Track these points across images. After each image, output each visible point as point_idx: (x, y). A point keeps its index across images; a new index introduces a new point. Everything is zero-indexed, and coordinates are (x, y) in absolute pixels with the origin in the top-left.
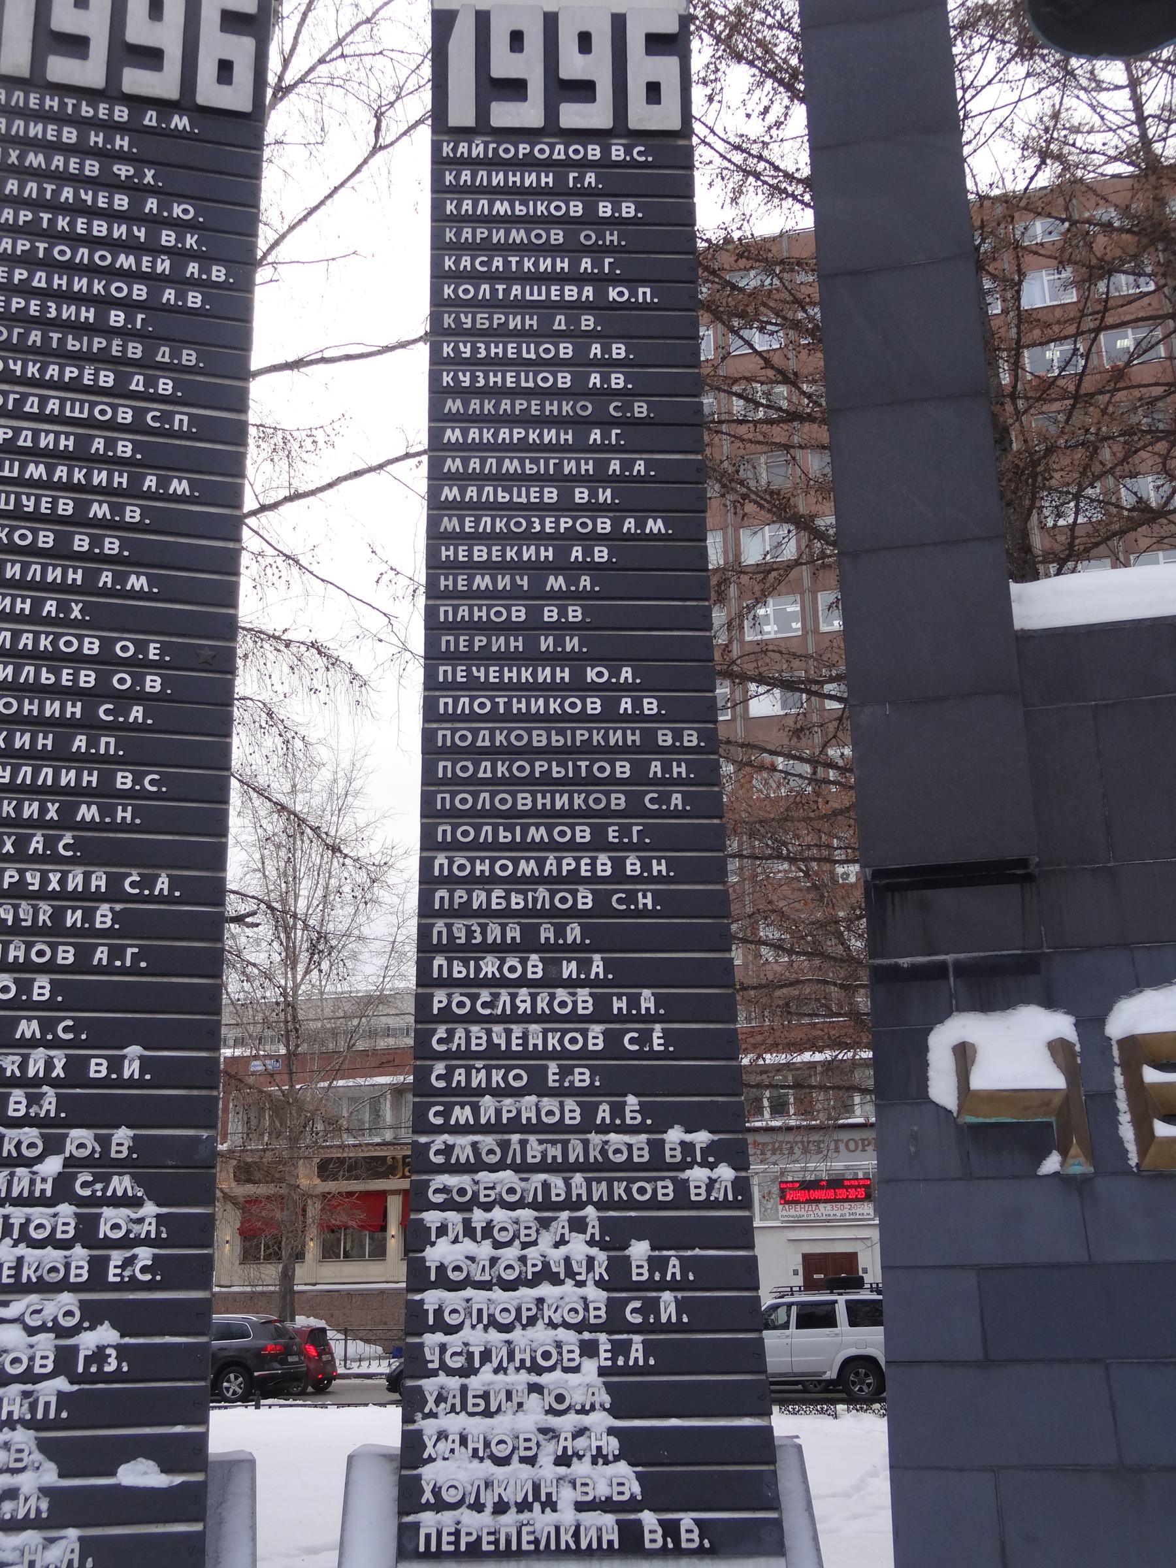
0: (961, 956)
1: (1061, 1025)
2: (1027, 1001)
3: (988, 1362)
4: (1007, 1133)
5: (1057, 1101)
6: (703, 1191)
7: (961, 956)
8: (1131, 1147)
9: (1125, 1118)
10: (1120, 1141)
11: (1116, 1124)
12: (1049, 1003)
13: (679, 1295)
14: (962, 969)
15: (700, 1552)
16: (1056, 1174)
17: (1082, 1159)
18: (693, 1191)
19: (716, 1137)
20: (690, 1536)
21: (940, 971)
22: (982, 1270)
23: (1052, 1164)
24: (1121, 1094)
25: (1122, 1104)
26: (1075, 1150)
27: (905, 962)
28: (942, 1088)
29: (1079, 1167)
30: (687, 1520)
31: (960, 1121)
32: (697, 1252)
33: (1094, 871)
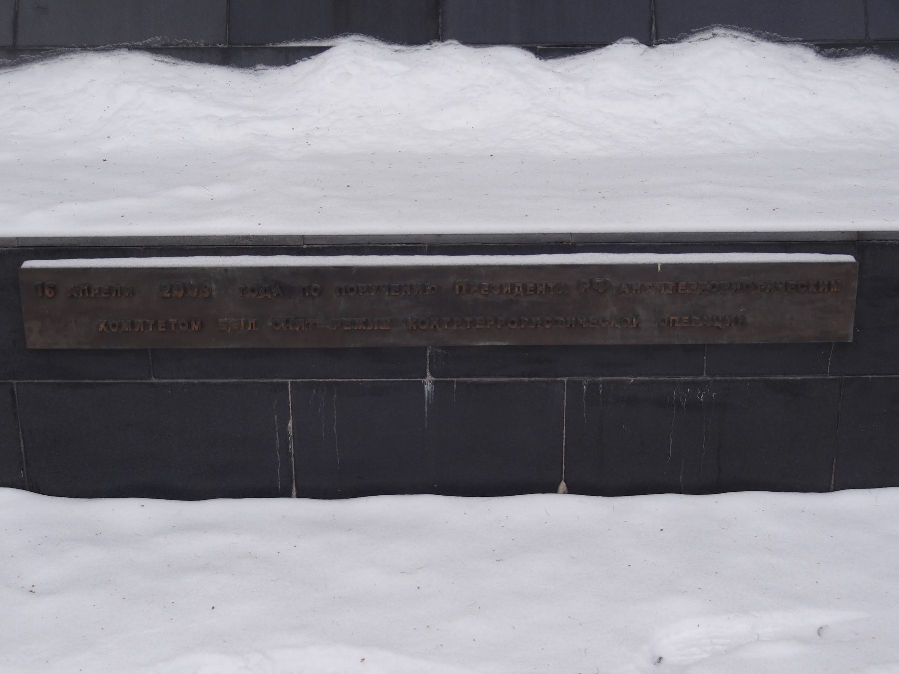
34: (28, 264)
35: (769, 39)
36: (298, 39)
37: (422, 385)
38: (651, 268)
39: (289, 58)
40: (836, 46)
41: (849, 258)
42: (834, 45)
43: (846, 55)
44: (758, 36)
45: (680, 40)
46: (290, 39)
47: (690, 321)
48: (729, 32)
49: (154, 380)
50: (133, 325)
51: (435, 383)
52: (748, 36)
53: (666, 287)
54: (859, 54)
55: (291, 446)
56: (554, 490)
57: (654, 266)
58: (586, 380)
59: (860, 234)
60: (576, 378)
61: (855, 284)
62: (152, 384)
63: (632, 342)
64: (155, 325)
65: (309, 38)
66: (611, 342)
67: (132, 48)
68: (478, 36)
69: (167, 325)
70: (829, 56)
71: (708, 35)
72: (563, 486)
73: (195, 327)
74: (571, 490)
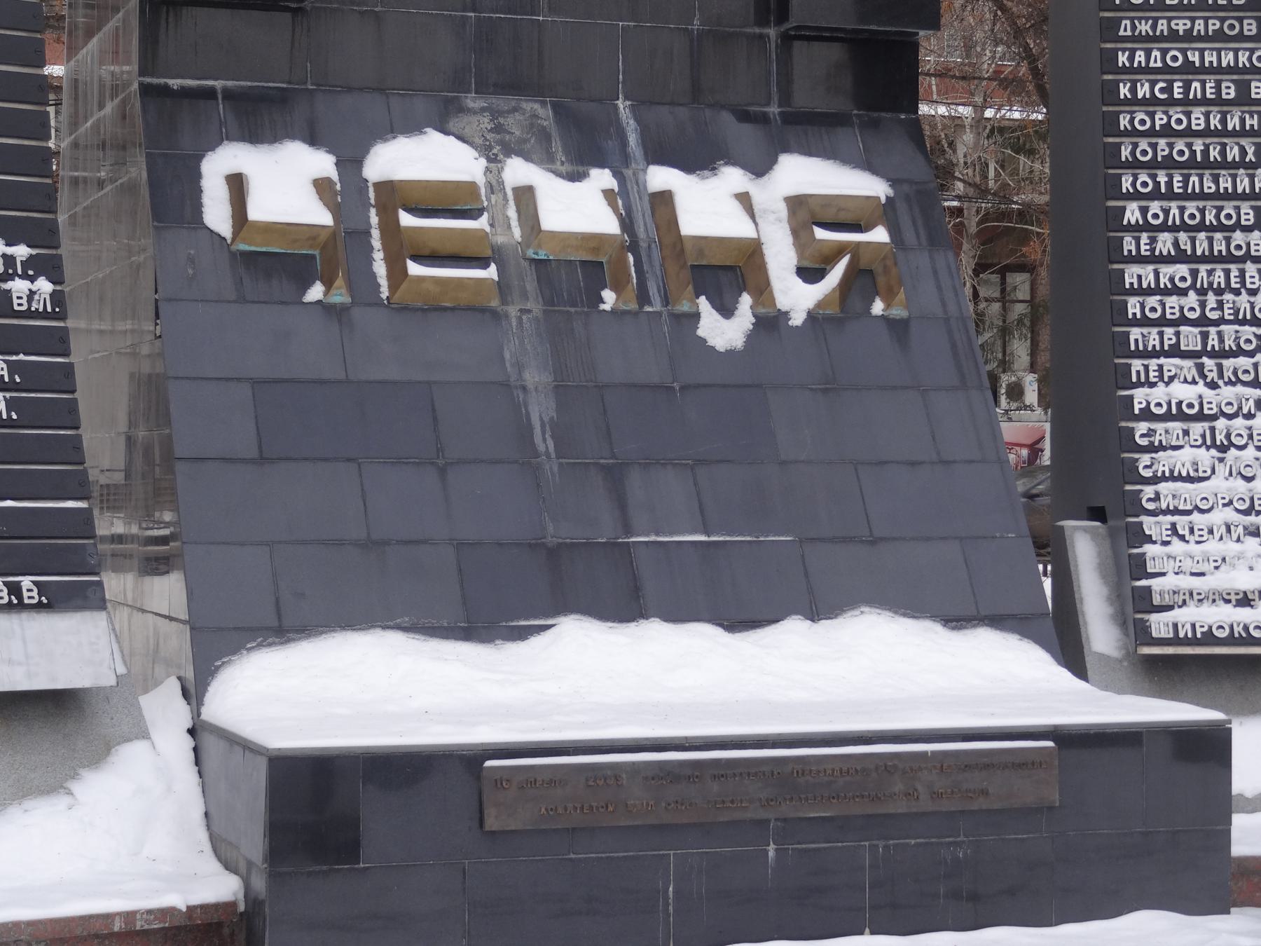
0: (230, 83)
1: (323, 163)
2: (293, 137)
3: (262, 459)
4: (276, 263)
5: (324, 236)
6: (24, 301)
7: (230, 83)
8: (383, 282)
9: (378, 256)
10: (373, 276)
11: (370, 260)
12: (313, 140)
13: (8, 395)
14: (229, 95)
15: (39, 606)
16: (319, 302)
17: (344, 291)
18: (16, 301)
19: (34, 252)
20: (30, 593)
21: (210, 94)
22: (256, 383)
23: (316, 292)
24: (375, 233)
25: (376, 243)
26: (339, 282)
27: (175, 83)
28: (217, 215)
29: (340, 297)
30: (26, 582)
31: (234, 248)
32: (21, 357)
33: (362, 13)
34: (489, 763)
35: (904, 615)
36: (527, 619)
37: (766, 852)
38: (923, 755)
39: (522, 634)
40: (958, 620)
41: (1050, 744)
42: (956, 620)
43: (965, 628)
44: (896, 613)
45: (836, 616)
46: (519, 618)
47: (952, 792)
48: (873, 610)
49: (572, 856)
50: (566, 809)
51: (776, 850)
52: (888, 613)
53: (935, 767)
54: (974, 626)
55: (671, 908)
56: (862, 934)
57: (925, 753)
58: (881, 844)
59: (1056, 727)
60: (875, 842)
61: (1056, 763)
62: (571, 860)
63: (914, 810)
64: (582, 808)
65: (536, 617)
66: (900, 811)
67: (385, 628)
68: (677, 614)
69: (591, 807)
70: (953, 628)
71: (857, 612)
72: (867, 930)
73: (611, 809)
74: (872, 933)
